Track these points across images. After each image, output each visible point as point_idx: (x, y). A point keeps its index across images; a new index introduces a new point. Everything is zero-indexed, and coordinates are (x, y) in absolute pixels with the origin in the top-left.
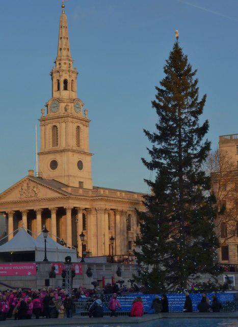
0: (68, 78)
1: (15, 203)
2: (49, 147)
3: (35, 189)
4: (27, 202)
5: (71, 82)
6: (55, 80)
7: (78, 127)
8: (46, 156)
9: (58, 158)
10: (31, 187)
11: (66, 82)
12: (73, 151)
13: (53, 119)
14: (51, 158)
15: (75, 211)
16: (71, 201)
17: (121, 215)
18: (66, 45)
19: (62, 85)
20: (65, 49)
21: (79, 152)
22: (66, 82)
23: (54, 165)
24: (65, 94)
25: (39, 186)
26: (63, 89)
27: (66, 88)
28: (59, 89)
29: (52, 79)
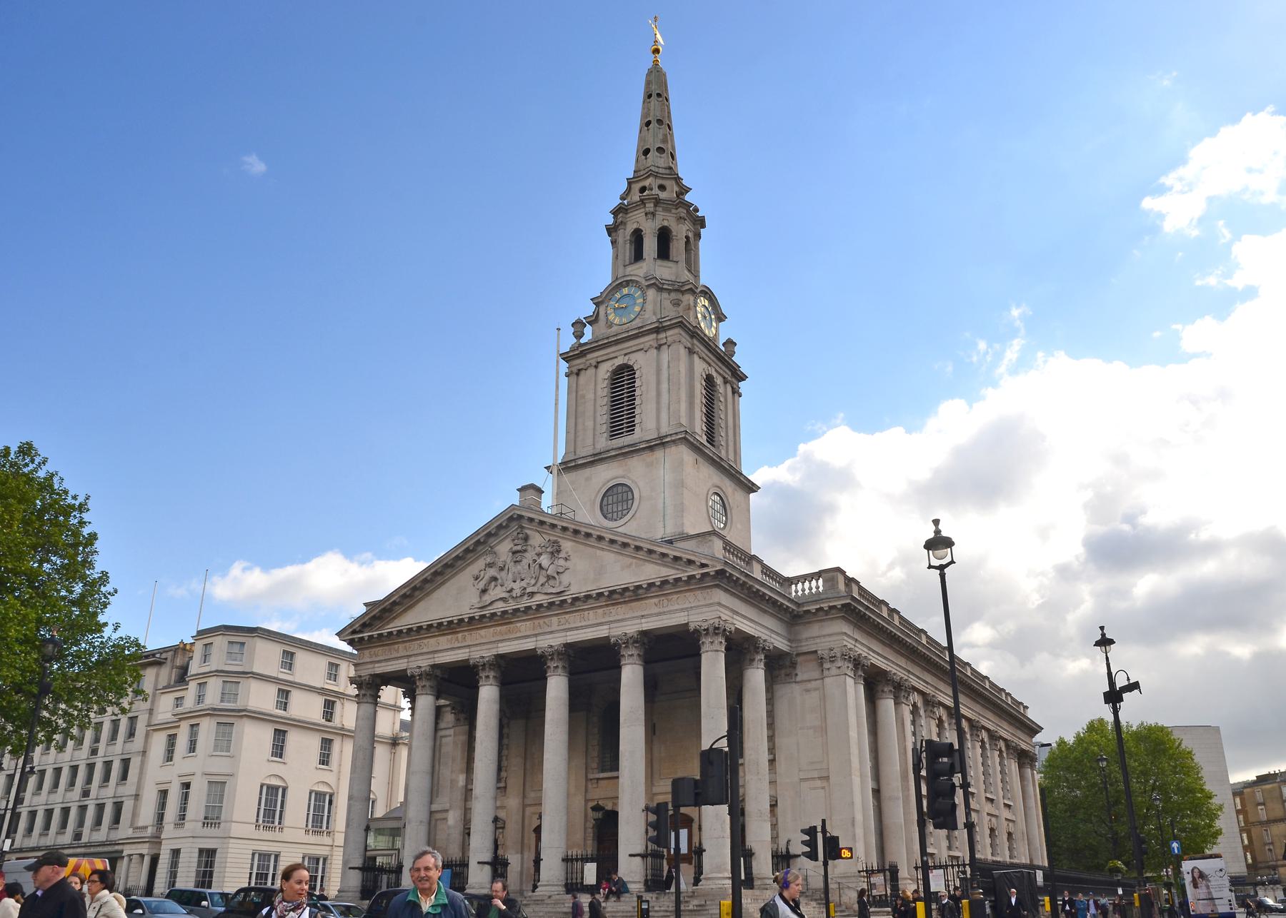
0: (671, 222)
2: (603, 443)
3: (545, 560)
4: (505, 618)
6: (625, 234)
7: (709, 380)
8: (587, 472)
9: (635, 472)
10: (530, 556)
11: (664, 237)
12: (696, 448)
13: (617, 342)
14: (605, 475)
15: (739, 650)
16: (720, 596)
18: (665, 141)
19: (650, 245)
20: (660, 150)
22: (664, 237)
25: (567, 545)
27: (664, 253)
28: (638, 256)
29: (614, 243)
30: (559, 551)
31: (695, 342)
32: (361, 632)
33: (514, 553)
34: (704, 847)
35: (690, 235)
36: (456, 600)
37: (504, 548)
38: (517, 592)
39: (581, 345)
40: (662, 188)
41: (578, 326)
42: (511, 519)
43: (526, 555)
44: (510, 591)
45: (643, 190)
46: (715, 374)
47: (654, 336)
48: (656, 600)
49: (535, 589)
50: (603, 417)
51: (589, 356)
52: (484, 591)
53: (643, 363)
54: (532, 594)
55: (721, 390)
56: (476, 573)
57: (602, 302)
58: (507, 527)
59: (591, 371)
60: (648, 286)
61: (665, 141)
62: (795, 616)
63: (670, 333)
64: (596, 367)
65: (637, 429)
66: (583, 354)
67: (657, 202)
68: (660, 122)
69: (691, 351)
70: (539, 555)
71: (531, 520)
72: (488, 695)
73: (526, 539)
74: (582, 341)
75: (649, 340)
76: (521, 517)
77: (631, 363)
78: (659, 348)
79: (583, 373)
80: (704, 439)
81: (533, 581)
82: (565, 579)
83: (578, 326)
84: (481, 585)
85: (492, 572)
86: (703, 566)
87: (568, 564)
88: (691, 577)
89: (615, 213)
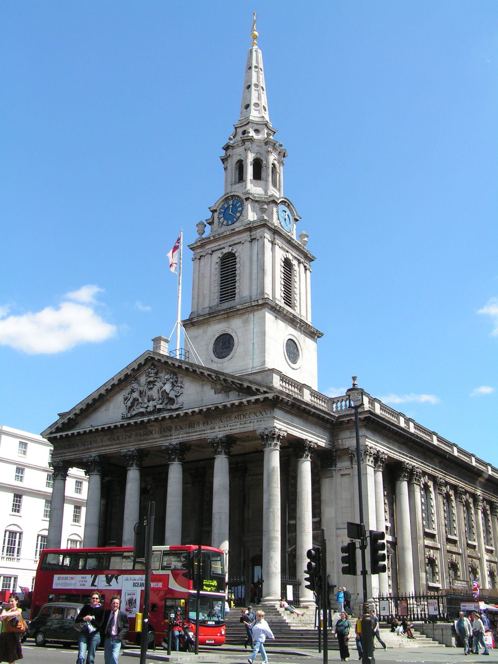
1: (109, 432)
3: (167, 387)
5: (271, 166)
7: (287, 263)
9: (234, 326)
10: (159, 384)
16: (278, 413)
17: (410, 484)
20: (256, 105)
21: (293, 321)
22: (258, 165)
23: (224, 345)
24: (254, 189)
26: (252, 178)
27: (257, 176)
28: (241, 178)
29: (226, 169)
30: (176, 382)
31: (276, 237)
32: (55, 432)
33: (150, 383)
34: (264, 579)
35: (276, 162)
36: (113, 413)
37: (143, 379)
38: (151, 409)
39: (203, 239)
40: (257, 131)
41: (201, 225)
42: (147, 360)
43: (156, 383)
44: (147, 408)
45: (244, 132)
46: (291, 258)
47: (248, 233)
48: (236, 414)
49: (161, 406)
50: (216, 289)
51: (207, 247)
52: (130, 408)
53: (243, 253)
54: (160, 411)
55: (296, 268)
56: (127, 395)
57: (216, 211)
58: (145, 364)
59: (207, 258)
60: (247, 199)
61: (259, 98)
62: (331, 425)
63: (259, 231)
64: (211, 254)
65: (237, 297)
66: (202, 246)
67: (251, 140)
68: (256, 85)
69: (273, 243)
70: (164, 384)
71: (159, 360)
72: (133, 476)
73: (156, 374)
74: (204, 236)
75: (245, 236)
76: (153, 358)
77: (234, 252)
78: (252, 240)
79: (202, 258)
80: (281, 303)
81: (160, 401)
82: (180, 399)
83: (201, 225)
84: (129, 404)
85: (136, 395)
86: (265, 392)
87: (182, 390)
88: (257, 400)
89: (227, 148)
